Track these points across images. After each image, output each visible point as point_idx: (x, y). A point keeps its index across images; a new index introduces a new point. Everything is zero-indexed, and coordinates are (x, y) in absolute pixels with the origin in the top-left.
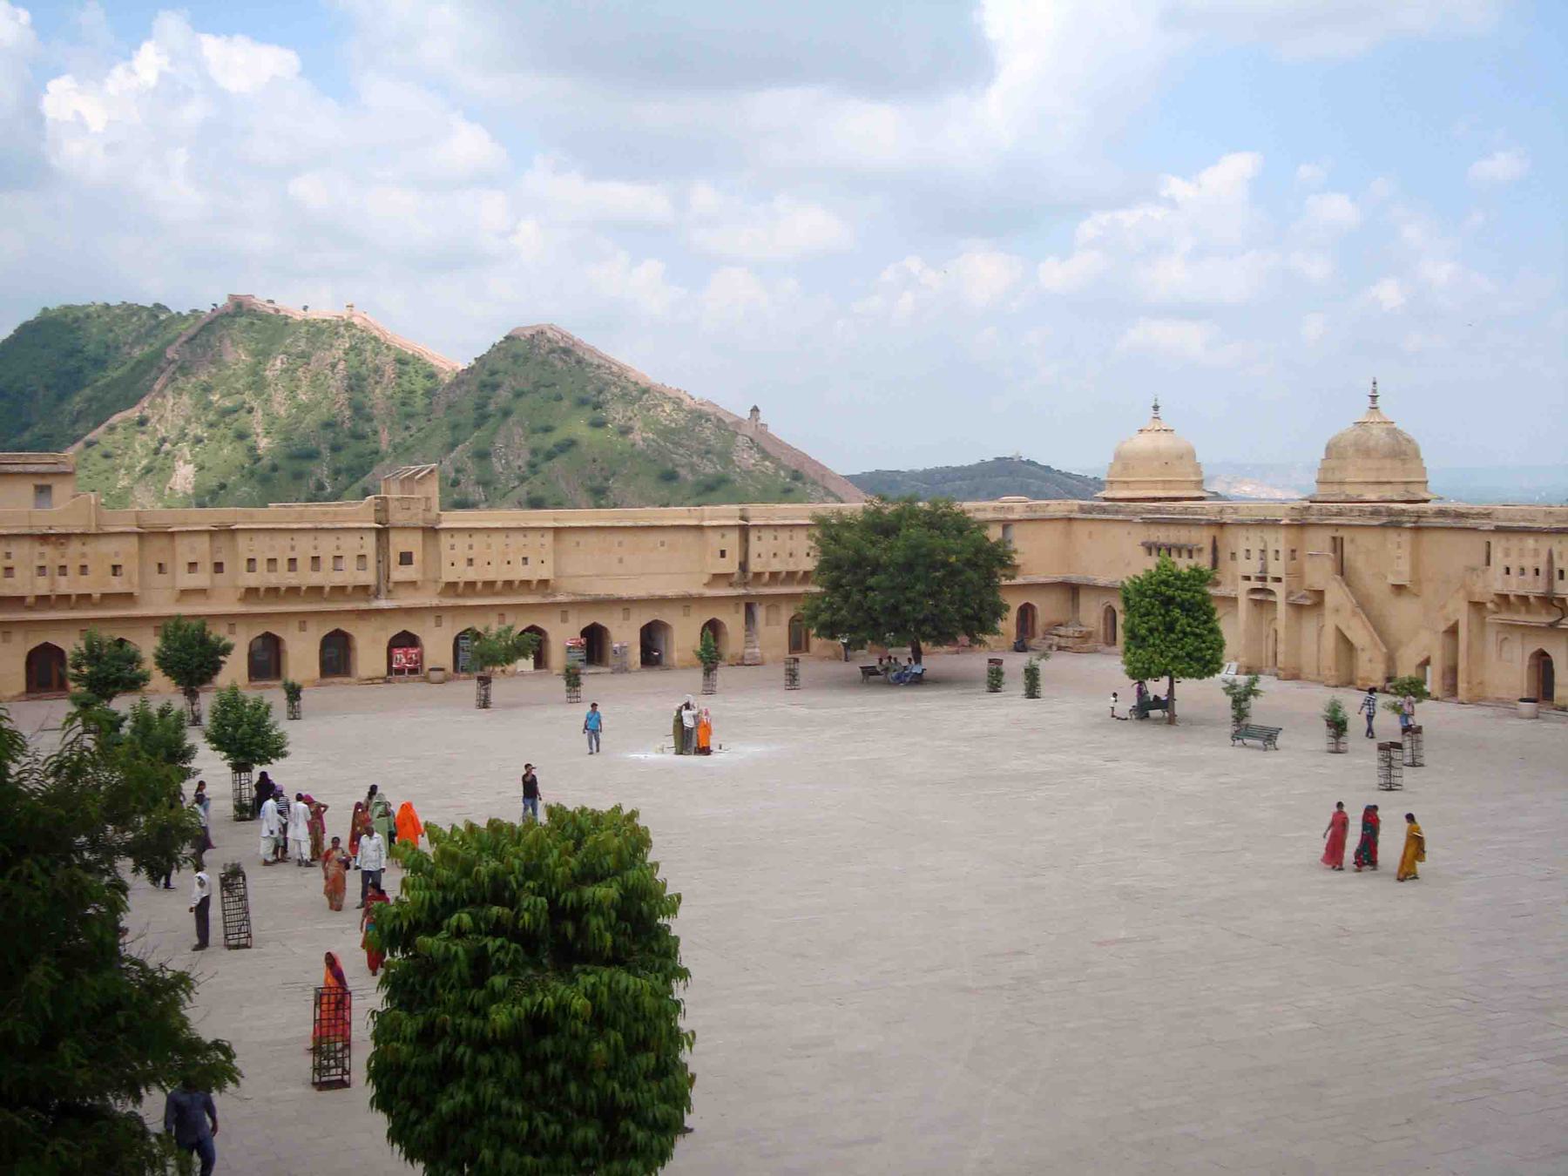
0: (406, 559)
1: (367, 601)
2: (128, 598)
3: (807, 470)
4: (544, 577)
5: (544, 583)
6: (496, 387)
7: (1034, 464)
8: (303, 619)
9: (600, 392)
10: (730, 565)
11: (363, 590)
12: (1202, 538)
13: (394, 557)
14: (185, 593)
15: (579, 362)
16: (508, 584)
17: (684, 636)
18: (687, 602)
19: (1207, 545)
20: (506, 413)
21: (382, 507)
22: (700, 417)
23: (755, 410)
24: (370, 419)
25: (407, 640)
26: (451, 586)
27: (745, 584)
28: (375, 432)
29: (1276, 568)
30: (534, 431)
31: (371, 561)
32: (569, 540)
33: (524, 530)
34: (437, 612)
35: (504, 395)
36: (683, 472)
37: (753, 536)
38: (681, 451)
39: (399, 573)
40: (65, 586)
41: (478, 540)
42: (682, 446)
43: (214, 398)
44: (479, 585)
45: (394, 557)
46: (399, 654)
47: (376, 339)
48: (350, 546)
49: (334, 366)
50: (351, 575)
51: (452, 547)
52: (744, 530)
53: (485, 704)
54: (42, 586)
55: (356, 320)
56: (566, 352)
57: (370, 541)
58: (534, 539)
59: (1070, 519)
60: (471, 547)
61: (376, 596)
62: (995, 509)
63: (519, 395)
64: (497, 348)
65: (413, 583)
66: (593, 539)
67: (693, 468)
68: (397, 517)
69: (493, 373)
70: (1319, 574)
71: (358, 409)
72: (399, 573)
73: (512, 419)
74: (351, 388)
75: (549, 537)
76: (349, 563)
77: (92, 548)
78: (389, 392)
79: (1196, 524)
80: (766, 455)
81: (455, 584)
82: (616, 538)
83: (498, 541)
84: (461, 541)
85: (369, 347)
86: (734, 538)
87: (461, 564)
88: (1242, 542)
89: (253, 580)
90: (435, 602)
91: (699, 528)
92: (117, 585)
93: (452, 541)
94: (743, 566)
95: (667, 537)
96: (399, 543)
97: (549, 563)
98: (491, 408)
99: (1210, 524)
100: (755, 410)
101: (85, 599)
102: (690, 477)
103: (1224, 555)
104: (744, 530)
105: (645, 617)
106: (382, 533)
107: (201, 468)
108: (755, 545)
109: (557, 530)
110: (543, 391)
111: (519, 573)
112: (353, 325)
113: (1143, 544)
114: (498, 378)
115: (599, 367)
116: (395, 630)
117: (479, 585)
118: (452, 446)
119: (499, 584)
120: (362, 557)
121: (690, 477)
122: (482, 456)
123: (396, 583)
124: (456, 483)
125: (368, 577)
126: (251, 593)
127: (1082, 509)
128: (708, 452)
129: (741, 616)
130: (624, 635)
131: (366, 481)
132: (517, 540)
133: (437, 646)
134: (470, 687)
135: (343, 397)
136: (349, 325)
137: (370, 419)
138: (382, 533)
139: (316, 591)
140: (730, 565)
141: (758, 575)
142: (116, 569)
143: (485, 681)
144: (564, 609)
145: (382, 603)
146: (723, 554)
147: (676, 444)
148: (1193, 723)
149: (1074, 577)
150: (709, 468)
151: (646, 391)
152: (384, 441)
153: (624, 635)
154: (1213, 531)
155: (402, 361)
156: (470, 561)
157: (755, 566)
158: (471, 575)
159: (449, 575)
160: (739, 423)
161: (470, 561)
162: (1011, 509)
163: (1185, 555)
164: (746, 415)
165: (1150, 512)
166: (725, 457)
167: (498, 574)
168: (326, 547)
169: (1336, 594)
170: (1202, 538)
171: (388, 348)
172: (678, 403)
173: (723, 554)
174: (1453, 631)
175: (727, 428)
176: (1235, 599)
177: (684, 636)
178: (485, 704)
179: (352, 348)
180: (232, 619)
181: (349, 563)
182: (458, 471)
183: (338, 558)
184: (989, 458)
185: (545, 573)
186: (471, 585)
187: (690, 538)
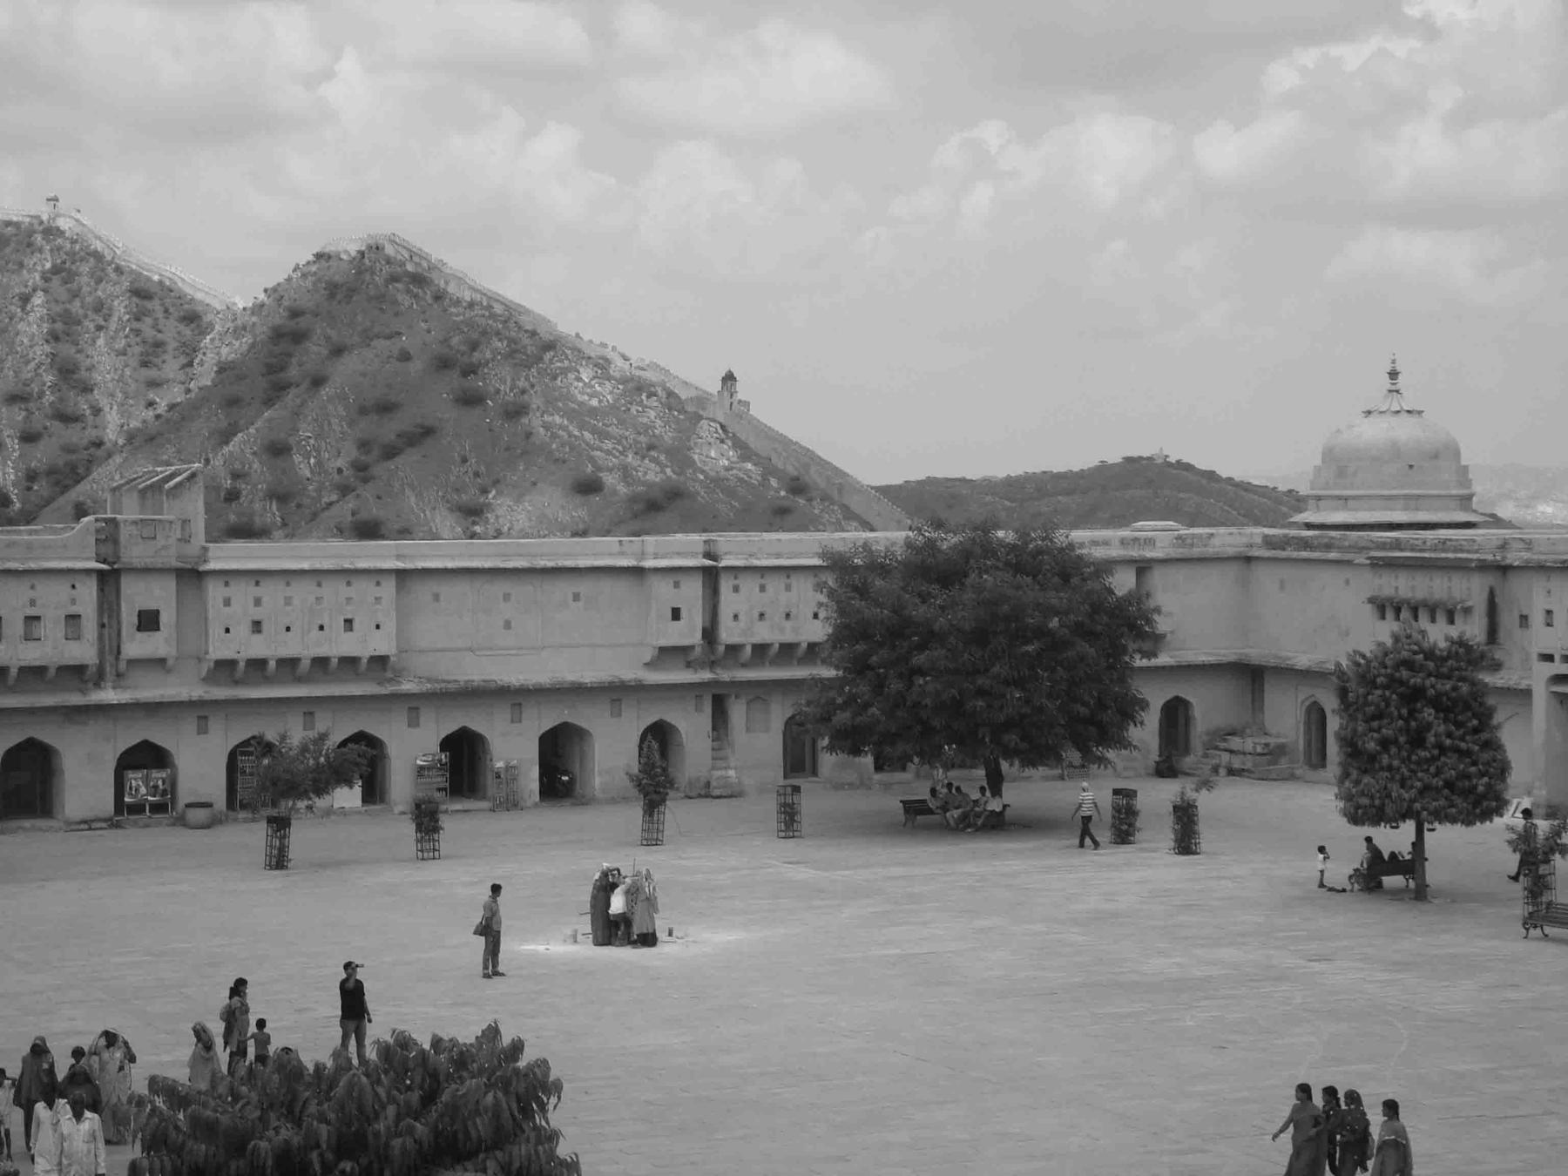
0: (148, 621)
1: (83, 692)
3: (814, 477)
4: (382, 650)
5: (380, 661)
6: (299, 337)
7: (1188, 467)
9: (474, 346)
10: (688, 633)
11: (75, 673)
12: (1472, 590)
13: (129, 618)
15: (439, 297)
16: (321, 662)
17: (612, 749)
18: (616, 693)
19: (1479, 602)
20: (318, 382)
21: (109, 535)
22: (639, 389)
23: (729, 378)
24: (87, 389)
25: (148, 756)
26: (225, 667)
27: (712, 665)
28: (97, 411)
30: (363, 411)
31: (90, 626)
32: (422, 591)
33: (349, 574)
34: (201, 711)
35: (315, 349)
36: (609, 479)
37: (725, 585)
38: (608, 445)
39: (137, 645)
41: (272, 592)
42: (608, 436)
44: (272, 664)
45: (129, 618)
46: (135, 779)
47: (98, 256)
48: (53, 600)
49: (25, 299)
50: (53, 649)
51: (227, 602)
52: (711, 576)
53: (279, 861)
55: (63, 224)
56: (419, 280)
57: (88, 593)
58: (364, 587)
59: (1248, 560)
60: (258, 602)
61: (99, 680)
62: (1123, 542)
63: (338, 351)
65: (161, 662)
66: (461, 587)
67: (626, 473)
68: (134, 552)
69: (295, 314)
71: (67, 372)
72: (137, 645)
73: (326, 391)
74: (54, 337)
75: (389, 587)
76: (52, 629)
78: (121, 344)
80: (745, 452)
81: (229, 664)
82: (500, 587)
83: (303, 592)
84: (242, 593)
85: (85, 268)
86: (693, 590)
87: (242, 630)
88: (1536, 596)
90: (198, 692)
91: (638, 572)
93: (227, 592)
94: (710, 634)
95: (585, 586)
96: (136, 595)
97: (390, 626)
98: (293, 372)
99: (1483, 567)
100: (729, 378)
102: (622, 489)
103: (1508, 620)
104: (711, 576)
105: (544, 719)
106: (108, 579)
108: (729, 602)
109: (401, 574)
110: (380, 344)
112: (60, 233)
113: (1371, 600)
114: (303, 322)
115: (471, 305)
116: (128, 737)
117: (272, 664)
118: (226, 437)
119: (305, 665)
120: (73, 619)
121: (622, 489)
122: (278, 450)
123: (132, 662)
124: (232, 496)
125: (84, 652)
127: (1269, 542)
128: (651, 447)
129: (705, 719)
130: (513, 748)
131: (79, 492)
132: (334, 591)
133: (200, 765)
134: (253, 835)
135: (41, 351)
136: (51, 232)
137: (87, 389)
138: (108, 579)
140: (688, 633)
141: (733, 649)
143: (280, 824)
144: (413, 705)
145: (109, 695)
146: (676, 614)
148: (1459, 899)
149: (1256, 653)
150: (652, 474)
151: (550, 346)
152: (112, 426)
153: (513, 748)
154: (1489, 580)
155: (142, 292)
156: (257, 626)
157: (729, 633)
158: (258, 647)
159: (220, 649)
160: (702, 400)
161: (257, 626)
162: (1150, 542)
163: (1441, 618)
164: (713, 386)
165: (1382, 546)
166: (680, 456)
167: (303, 646)
170: (1472, 590)
171: (119, 270)
172: (602, 366)
173: (676, 614)
175: (684, 411)
176: (1527, 694)
177: (612, 749)
178: (279, 861)
179: (56, 270)
181: (52, 629)
182: (236, 476)
183: (32, 620)
184: (1114, 457)
185: (382, 644)
186: (258, 664)
187: (621, 586)
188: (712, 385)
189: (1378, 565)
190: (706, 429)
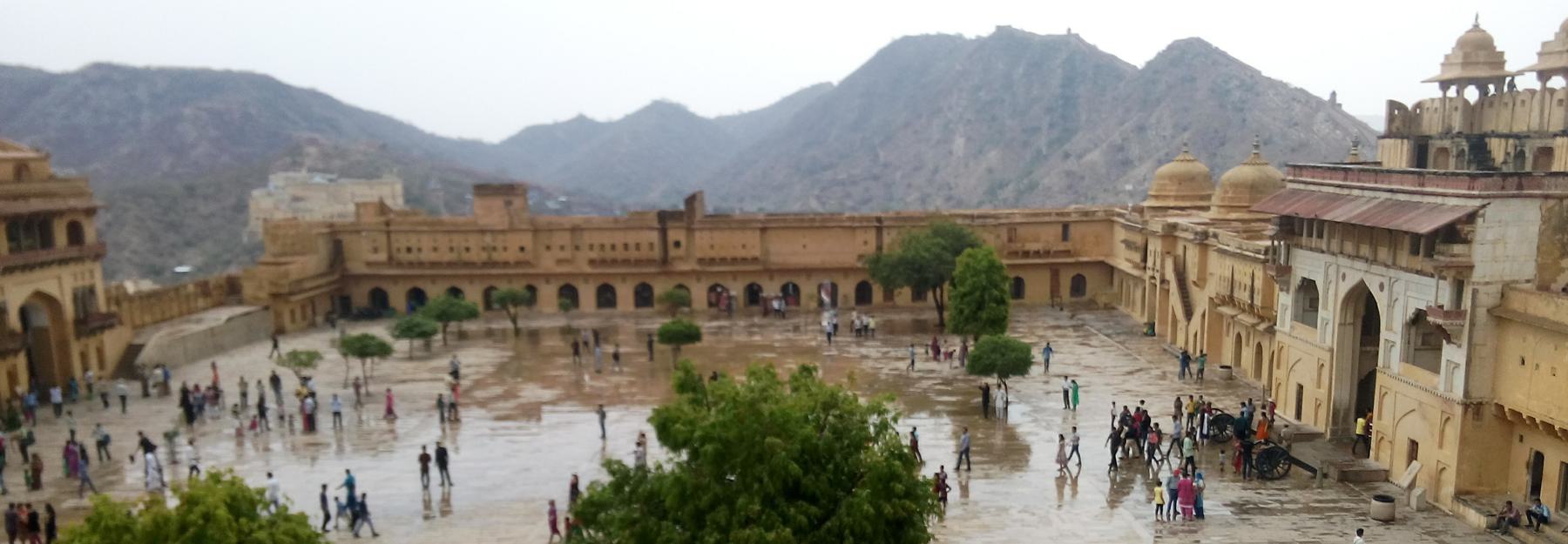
2: (526, 263)
8: (624, 277)
11: (650, 262)
14: (560, 262)
16: (734, 260)
23: (1334, 94)
26: (701, 261)
37: (885, 233)
40: (498, 256)
43: (981, 94)
50: (644, 253)
54: (484, 256)
77: (509, 236)
80: (1336, 125)
89: (594, 255)
92: (521, 256)
96: (673, 235)
100: (1334, 94)
101: (506, 264)
107: (969, 139)
111: (741, 253)
126: (592, 262)
131: (1067, 147)
139: (626, 262)
142: (522, 249)
159: (699, 255)
160: (1319, 101)
162: (1068, 214)
164: (1326, 97)
167: (729, 254)
168: (632, 238)
169: (1173, 287)
180: (586, 277)
181: (645, 248)
185: (756, 253)
188: (1326, 97)
190: (1321, 116)
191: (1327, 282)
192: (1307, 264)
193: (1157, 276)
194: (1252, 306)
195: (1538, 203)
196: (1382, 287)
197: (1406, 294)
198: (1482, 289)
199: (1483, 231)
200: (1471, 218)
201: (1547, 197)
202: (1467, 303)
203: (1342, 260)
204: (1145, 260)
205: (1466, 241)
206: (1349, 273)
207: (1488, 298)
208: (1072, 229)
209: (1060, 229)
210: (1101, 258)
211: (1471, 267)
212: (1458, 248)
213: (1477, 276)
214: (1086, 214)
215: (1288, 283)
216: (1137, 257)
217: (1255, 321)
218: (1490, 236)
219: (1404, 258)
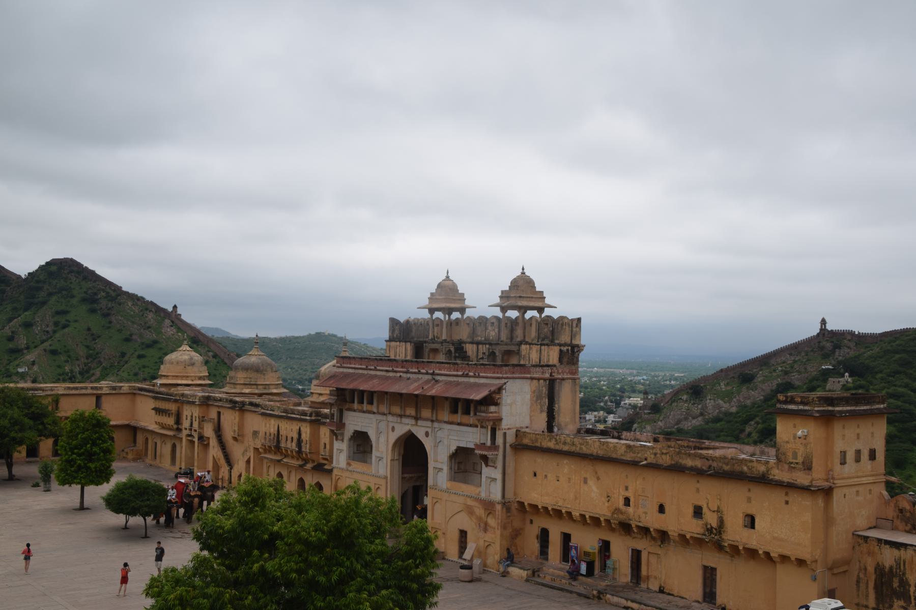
7: (335, 336)
9: (95, 294)
20: (44, 303)
23: (175, 307)
29: (196, 425)
63: (50, 294)
64: (41, 268)
69: (38, 282)
70: (209, 431)
79: (168, 400)
88: (187, 411)
100: (175, 307)
128: (149, 327)
147: (133, 322)
149: (133, 423)
162: (101, 388)
164: (170, 309)
169: (213, 442)
174: (248, 462)
182: (13, 332)
184: (313, 333)
188: (170, 309)
189: (155, 398)
191: (379, 433)
192: (355, 421)
193: (196, 435)
194: (300, 452)
195: (529, 381)
196: (427, 434)
197: (442, 441)
198: (507, 432)
199: (506, 398)
200: (500, 390)
201: (532, 379)
202: (499, 441)
203: (390, 418)
204: (178, 421)
205: (497, 404)
206: (396, 426)
207: (511, 439)
208: (103, 399)
209: (94, 399)
210: (127, 423)
211: (501, 420)
212: (492, 408)
213: (505, 424)
214: (114, 388)
215: (343, 434)
216: (170, 421)
217: (300, 462)
218: (509, 401)
219: (445, 415)
